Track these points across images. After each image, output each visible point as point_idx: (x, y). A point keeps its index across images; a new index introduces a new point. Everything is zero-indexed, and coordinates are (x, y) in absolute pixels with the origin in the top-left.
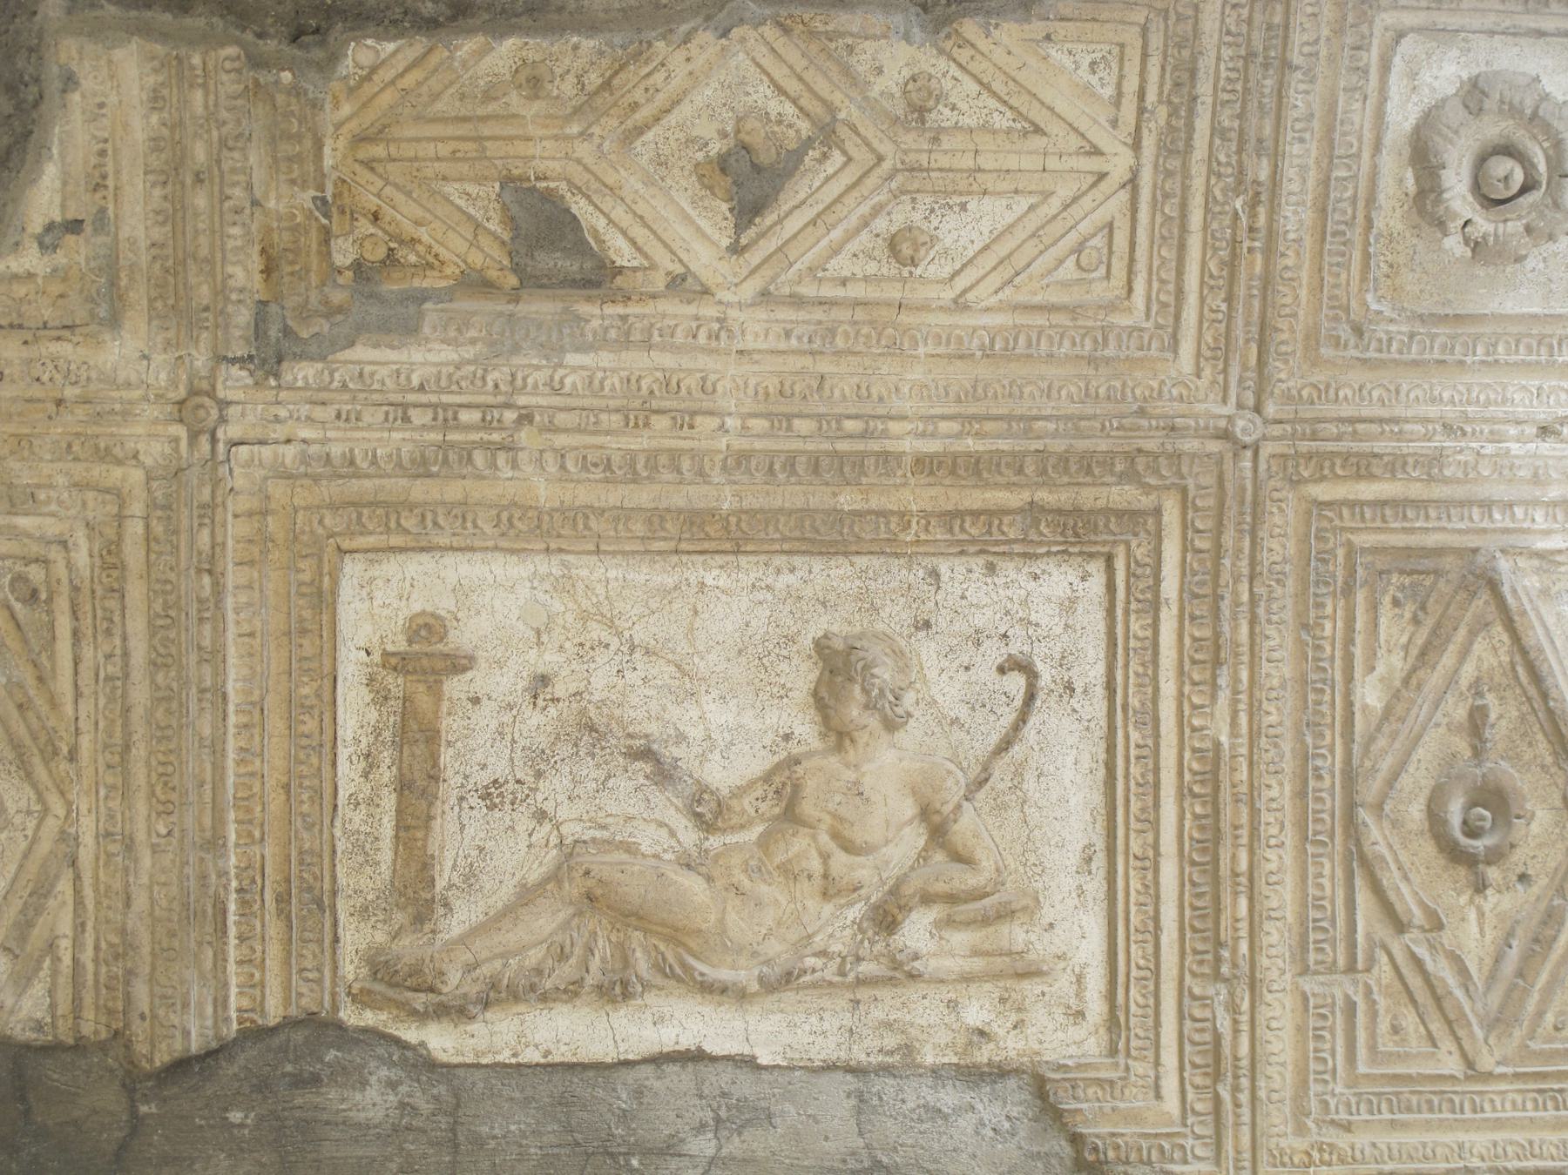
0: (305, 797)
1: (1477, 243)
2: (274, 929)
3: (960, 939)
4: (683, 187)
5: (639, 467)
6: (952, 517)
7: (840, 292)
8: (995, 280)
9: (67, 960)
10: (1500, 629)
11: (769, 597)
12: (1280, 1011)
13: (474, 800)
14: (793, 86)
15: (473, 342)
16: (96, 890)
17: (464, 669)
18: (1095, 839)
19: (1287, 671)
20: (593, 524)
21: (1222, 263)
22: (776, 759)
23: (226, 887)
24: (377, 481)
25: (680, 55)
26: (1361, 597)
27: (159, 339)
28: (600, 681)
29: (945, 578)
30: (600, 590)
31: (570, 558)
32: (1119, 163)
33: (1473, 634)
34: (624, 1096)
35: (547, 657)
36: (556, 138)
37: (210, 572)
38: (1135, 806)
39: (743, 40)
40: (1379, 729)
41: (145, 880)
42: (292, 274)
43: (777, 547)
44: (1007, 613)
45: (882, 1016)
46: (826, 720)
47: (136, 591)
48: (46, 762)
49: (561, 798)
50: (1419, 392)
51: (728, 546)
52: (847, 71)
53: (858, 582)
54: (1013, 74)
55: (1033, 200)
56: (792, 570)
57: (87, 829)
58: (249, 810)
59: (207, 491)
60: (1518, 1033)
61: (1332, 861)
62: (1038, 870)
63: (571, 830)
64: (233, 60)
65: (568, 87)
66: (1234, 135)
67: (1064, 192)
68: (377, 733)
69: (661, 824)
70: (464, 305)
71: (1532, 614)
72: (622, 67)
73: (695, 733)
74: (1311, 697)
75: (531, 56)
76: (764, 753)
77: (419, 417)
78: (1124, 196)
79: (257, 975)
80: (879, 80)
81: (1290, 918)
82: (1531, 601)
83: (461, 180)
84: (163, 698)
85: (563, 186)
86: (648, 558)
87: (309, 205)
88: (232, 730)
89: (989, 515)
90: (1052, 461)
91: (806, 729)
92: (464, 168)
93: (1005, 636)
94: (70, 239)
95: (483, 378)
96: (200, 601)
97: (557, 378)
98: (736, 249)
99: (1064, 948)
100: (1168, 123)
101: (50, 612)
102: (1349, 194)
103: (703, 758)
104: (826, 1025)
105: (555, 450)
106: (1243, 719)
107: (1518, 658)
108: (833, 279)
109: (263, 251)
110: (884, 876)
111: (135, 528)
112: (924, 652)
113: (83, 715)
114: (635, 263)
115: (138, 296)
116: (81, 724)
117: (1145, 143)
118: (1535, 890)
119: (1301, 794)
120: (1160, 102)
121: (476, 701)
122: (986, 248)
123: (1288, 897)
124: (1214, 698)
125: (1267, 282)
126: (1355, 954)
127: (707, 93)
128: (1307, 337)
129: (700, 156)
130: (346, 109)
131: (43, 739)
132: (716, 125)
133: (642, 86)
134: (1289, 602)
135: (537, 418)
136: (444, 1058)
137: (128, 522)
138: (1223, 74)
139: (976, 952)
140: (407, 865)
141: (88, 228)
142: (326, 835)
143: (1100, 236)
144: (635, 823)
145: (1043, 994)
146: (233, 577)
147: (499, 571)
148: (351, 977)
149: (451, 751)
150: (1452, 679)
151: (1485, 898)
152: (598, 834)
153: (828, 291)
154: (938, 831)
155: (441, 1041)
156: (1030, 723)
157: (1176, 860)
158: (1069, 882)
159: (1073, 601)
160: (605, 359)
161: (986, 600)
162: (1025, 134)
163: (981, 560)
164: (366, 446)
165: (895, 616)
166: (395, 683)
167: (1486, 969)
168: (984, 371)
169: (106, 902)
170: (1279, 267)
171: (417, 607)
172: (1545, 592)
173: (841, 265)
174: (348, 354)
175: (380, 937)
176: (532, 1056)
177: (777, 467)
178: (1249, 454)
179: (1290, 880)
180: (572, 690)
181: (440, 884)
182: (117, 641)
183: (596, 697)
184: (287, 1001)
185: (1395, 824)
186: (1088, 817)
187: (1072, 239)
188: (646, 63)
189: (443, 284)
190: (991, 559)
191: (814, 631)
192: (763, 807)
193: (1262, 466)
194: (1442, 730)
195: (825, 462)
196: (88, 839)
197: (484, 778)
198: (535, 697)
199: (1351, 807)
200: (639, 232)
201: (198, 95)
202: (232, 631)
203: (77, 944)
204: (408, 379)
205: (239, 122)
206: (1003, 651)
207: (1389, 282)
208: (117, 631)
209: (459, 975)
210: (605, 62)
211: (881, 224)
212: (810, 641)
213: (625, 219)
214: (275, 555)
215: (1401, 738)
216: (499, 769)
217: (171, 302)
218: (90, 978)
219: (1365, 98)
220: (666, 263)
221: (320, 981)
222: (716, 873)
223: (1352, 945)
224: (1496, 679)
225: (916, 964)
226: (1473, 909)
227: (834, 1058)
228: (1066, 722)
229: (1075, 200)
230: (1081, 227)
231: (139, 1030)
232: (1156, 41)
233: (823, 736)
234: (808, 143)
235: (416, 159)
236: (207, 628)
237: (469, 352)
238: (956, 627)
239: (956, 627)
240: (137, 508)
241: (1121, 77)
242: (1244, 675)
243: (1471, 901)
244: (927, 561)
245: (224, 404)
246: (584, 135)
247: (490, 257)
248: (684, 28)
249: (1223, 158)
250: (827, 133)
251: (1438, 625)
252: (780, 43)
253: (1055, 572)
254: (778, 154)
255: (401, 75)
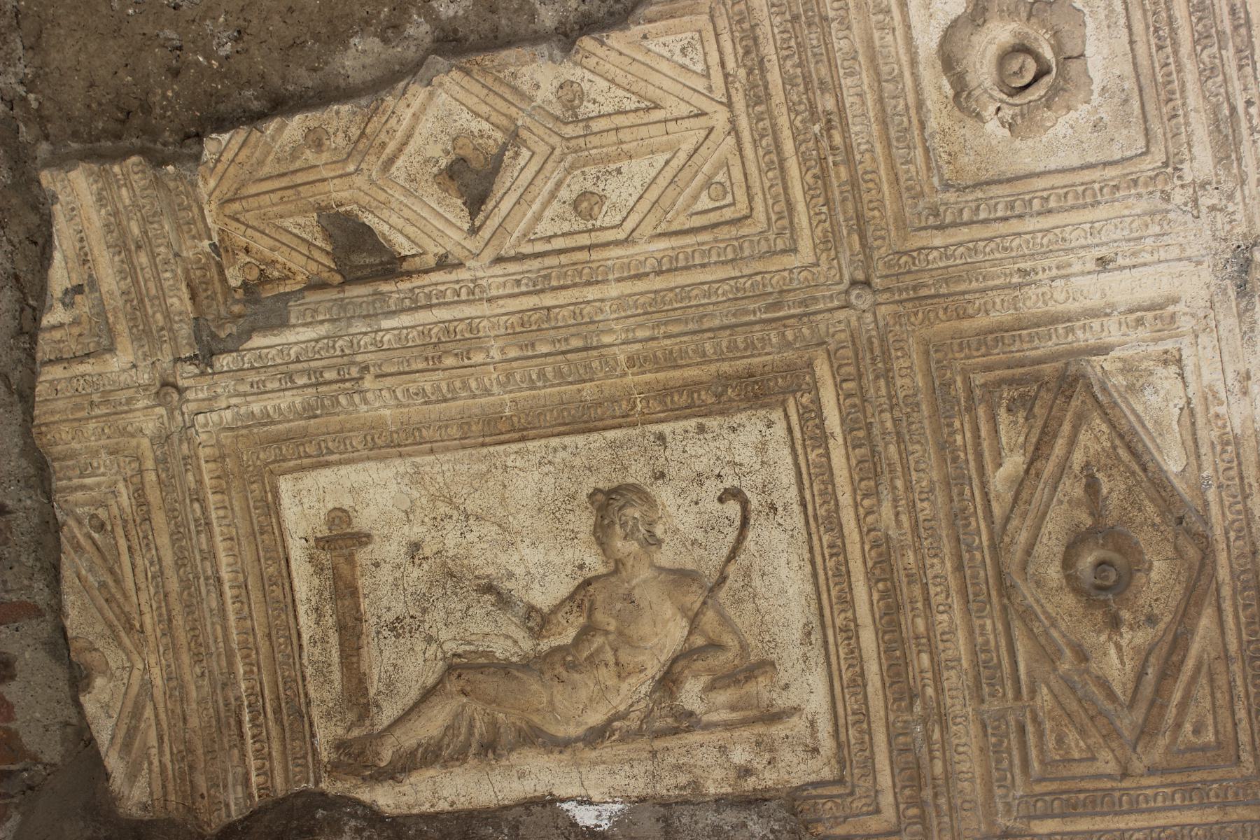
0: (282, 640)
1: (1010, 125)
2: (274, 731)
3: (722, 697)
4: (431, 193)
5: (445, 390)
6: (664, 392)
7: (548, 247)
8: (652, 220)
9: (156, 762)
10: (1098, 421)
11: (552, 469)
12: (966, 736)
13: (386, 633)
14: (484, 109)
15: (322, 322)
16: (167, 715)
17: (366, 544)
18: (811, 618)
19: (935, 475)
20: (424, 432)
21: (815, 177)
22: (576, 583)
23: (240, 706)
24: (287, 425)
25: (403, 103)
26: (981, 411)
27: (140, 353)
28: (451, 540)
29: (669, 439)
30: (440, 479)
31: (418, 460)
32: (720, 118)
33: (1076, 429)
34: (506, 831)
35: (415, 529)
36: (341, 176)
37: (197, 500)
38: (833, 593)
39: (441, 84)
40: (1012, 511)
41: (194, 706)
42: (207, 298)
43: (549, 431)
44: (718, 459)
45: (674, 761)
46: (604, 551)
47: (159, 518)
48: (128, 634)
49: (440, 625)
50: (992, 245)
51: (516, 435)
52: (515, 90)
53: (610, 451)
54: (627, 69)
55: (667, 156)
56: (565, 448)
57: (156, 673)
58: (248, 656)
59: (185, 446)
60: (1163, 742)
61: (992, 618)
62: (772, 645)
63: (450, 647)
64: (137, 165)
65: (340, 140)
66: (800, 80)
67: (687, 147)
68: (320, 593)
69: (507, 637)
70: (312, 297)
71: (1123, 406)
72: (369, 120)
73: (519, 571)
74: (955, 491)
75: (312, 124)
76: (567, 579)
77: (301, 381)
78: (731, 140)
79: (267, 764)
80: (539, 93)
81: (965, 664)
82: (1120, 395)
83: (291, 216)
84: (186, 584)
85: (355, 207)
86: (467, 452)
87: (208, 250)
88: (229, 601)
89: (691, 387)
90: (724, 344)
91: (595, 563)
92: (291, 207)
93: (719, 476)
94: (78, 298)
95: (334, 347)
96: (196, 520)
97: (378, 339)
98: (474, 231)
99: (798, 702)
100: (748, 80)
101: (114, 538)
102: (901, 106)
103: (527, 588)
104: (636, 771)
105: (389, 389)
106: (904, 518)
107: (1117, 442)
108: (542, 238)
109: (188, 285)
110: (663, 659)
111: (151, 477)
112: (663, 494)
113: (143, 602)
114: (413, 252)
115: (122, 327)
116: (143, 608)
117: (734, 99)
118: (1162, 626)
119: (959, 568)
120: (738, 66)
121: (377, 565)
122: (641, 197)
123: (962, 648)
124: (879, 502)
125: (854, 183)
126: (1020, 688)
127: (426, 126)
128: (896, 220)
129: (435, 170)
130: (212, 183)
131: (123, 620)
132: (440, 146)
133: (384, 130)
134: (926, 423)
135: (372, 369)
136: (388, 811)
137: (145, 474)
138: (778, 37)
139: (733, 708)
140: (349, 681)
141: (86, 289)
142: (298, 666)
143: (721, 173)
144: (490, 638)
145: (787, 737)
146: (212, 499)
147: (375, 476)
148: (326, 760)
149: (367, 601)
150: (1064, 466)
151: (1121, 635)
152: (468, 648)
153: (540, 247)
154: (694, 623)
155: (385, 798)
156: (749, 538)
157: (872, 627)
158: (797, 652)
159: (764, 444)
160: (405, 320)
161: (701, 451)
162: (648, 109)
163: (692, 423)
164: (273, 403)
165: (638, 473)
166: (325, 557)
167: (1129, 693)
168: (658, 283)
169: (173, 722)
170: (860, 172)
171: (330, 506)
172: (1131, 388)
173: (544, 228)
174: (249, 345)
175: (340, 731)
176: (443, 806)
177: (534, 377)
178: (869, 317)
179: (961, 635)
180: (435, 550)
181: (372, 692)
182: (154, 552)
183: (450, 554)
184: (287, 780)
185: (1038, 583)
186: (804, 602)
187: (700, 178)
188: (383, 113)
189: (298, 287)
190: (700, 420)
191: (587, 489)
192: (571, 618)
193: (881, 324)
194: (1065, 506)
195: (565, 370)
196: (158, 682)
197: (390, 617)
198: (413, 558)
199: (1000, 575)
200: (410, 230)
201: (124, 191)
202: (218, 538)
203: (161, 753)
204: (289, 355)
205: (153, 205)
206: (720, 486)
207: (951, 167)
208: (152, 546)
209: (390, 753)
210: (358, 119)
211: (564, 193)
212: (584, 497)
213: (400, 223)
214: (235, 483)
215: (1031, 515)
216: (399, 609)
217: (141, 327)
218: (170, 773)
219: (894, 29)
220: (433, 250)
221: (306, 766)
222: (545, 668)
223: (1017, 680)
224: (1102, 462)
225: (693, 719)
226: (1112, 645)
227: (644, 794)
228: (775, 532)
229: (696, 151)
230: (705, 169)
231: (202, 805)
232: (722, 23)
233: (605, 563)
234: (504, 148)
235: (260, 207)
236: (203, 535)
237: (322, 330)
238: (683, 473)
239: (683, 473)
240: (149, 464)
241: (705, 54)
242: (899, 483)
243: (1110, 638)
244: (656, 428)
245: (181, 391)
246: (358, 171)
247: (322, 263)
248: (402, 84)
249: (795, 98)
250: (514, 137)
251: (1045, 426)
252: (466, 81)
253: (748, 425)
254: (486, 159)
255: (237, 154)
